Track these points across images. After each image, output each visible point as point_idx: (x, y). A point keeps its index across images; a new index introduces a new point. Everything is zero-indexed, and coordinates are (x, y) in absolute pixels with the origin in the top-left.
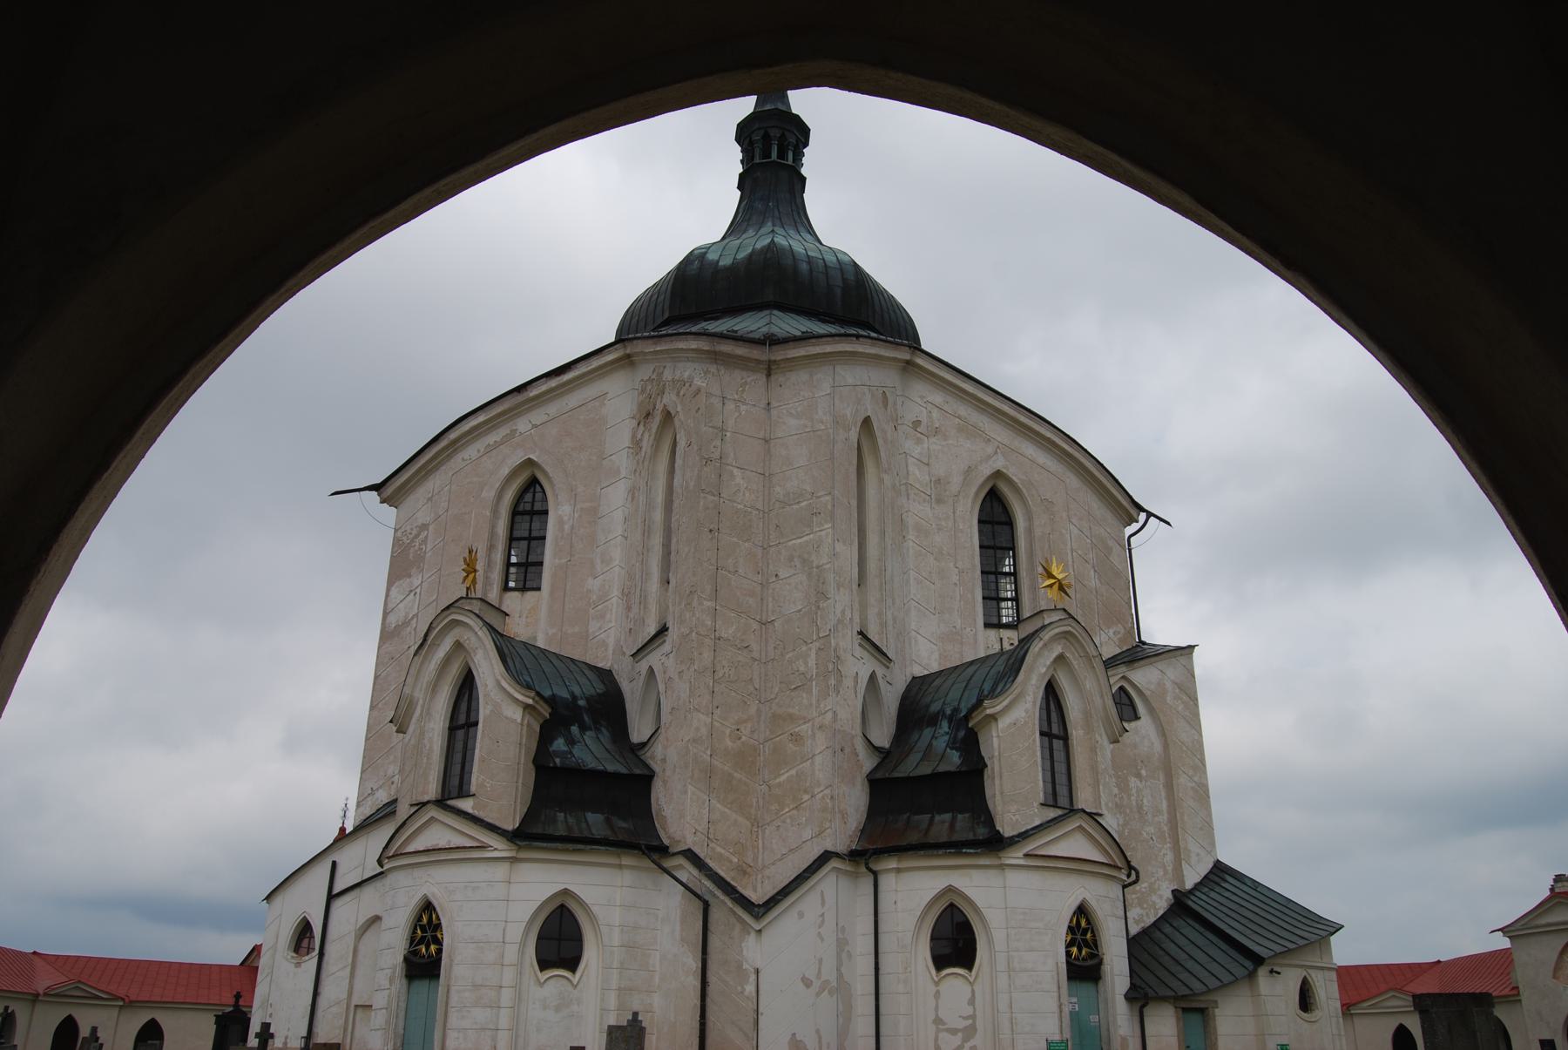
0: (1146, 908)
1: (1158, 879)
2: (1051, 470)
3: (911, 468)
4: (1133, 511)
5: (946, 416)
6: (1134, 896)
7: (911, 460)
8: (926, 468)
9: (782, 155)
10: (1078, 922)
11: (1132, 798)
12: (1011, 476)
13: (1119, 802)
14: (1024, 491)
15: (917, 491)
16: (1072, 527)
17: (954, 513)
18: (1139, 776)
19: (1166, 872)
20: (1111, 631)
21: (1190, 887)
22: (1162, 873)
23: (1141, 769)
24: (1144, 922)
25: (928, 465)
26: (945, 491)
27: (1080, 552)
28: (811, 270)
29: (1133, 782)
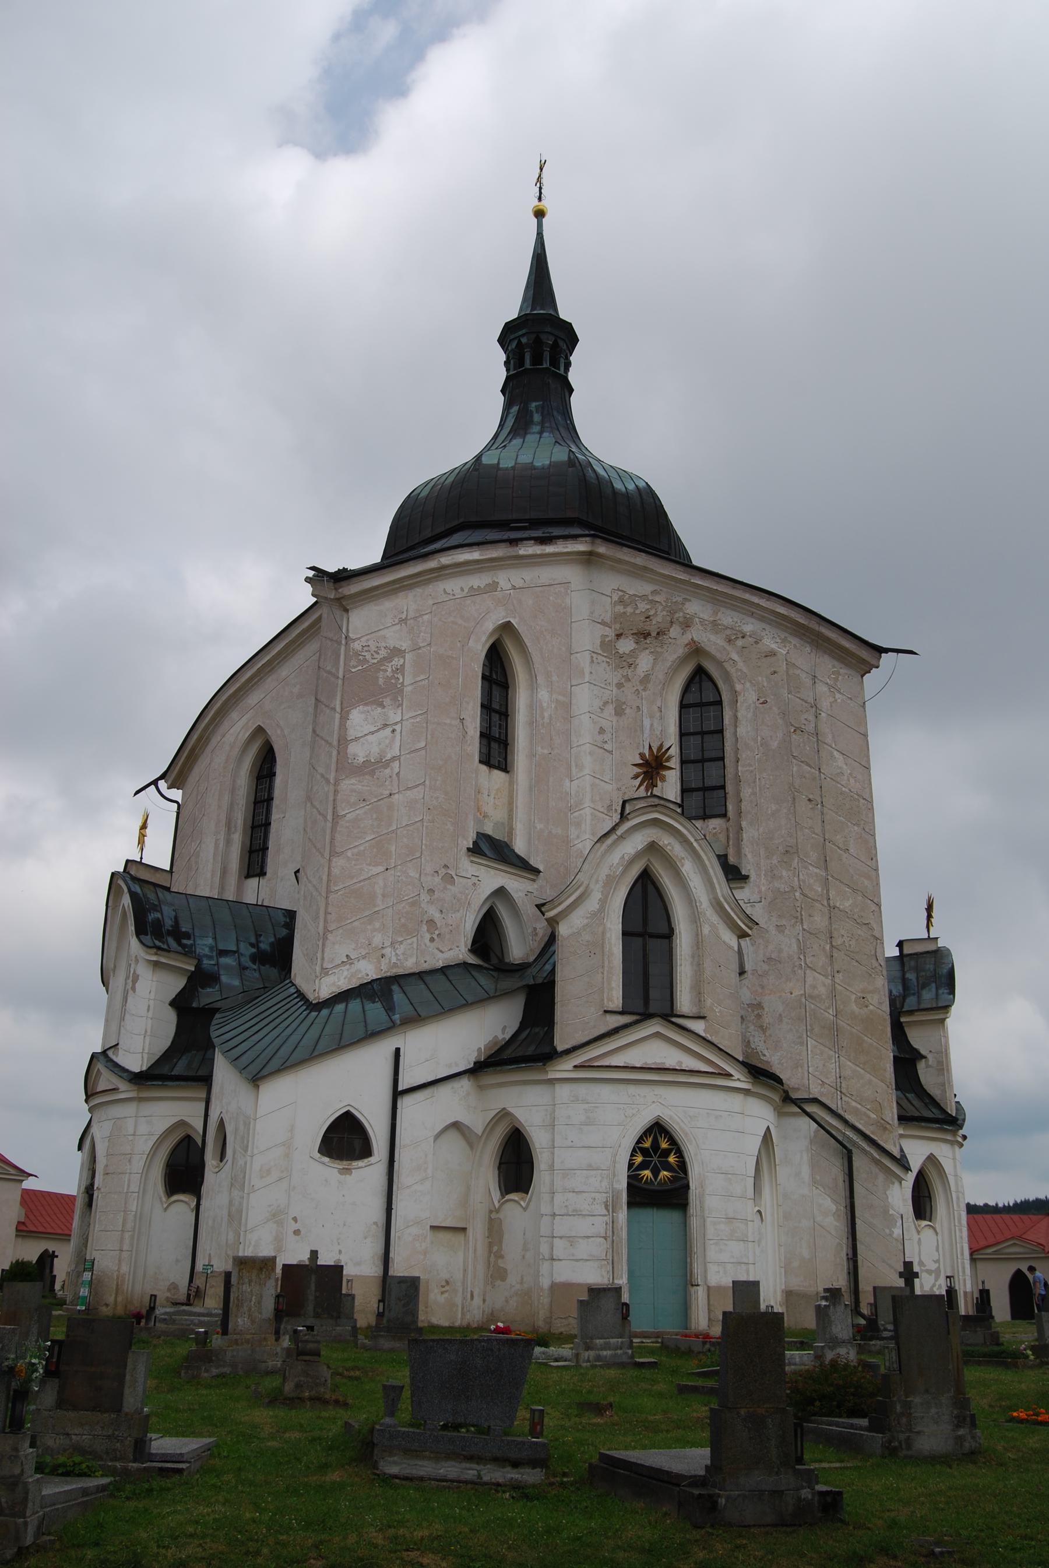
9: (537, 359)
10: (655, 1145)
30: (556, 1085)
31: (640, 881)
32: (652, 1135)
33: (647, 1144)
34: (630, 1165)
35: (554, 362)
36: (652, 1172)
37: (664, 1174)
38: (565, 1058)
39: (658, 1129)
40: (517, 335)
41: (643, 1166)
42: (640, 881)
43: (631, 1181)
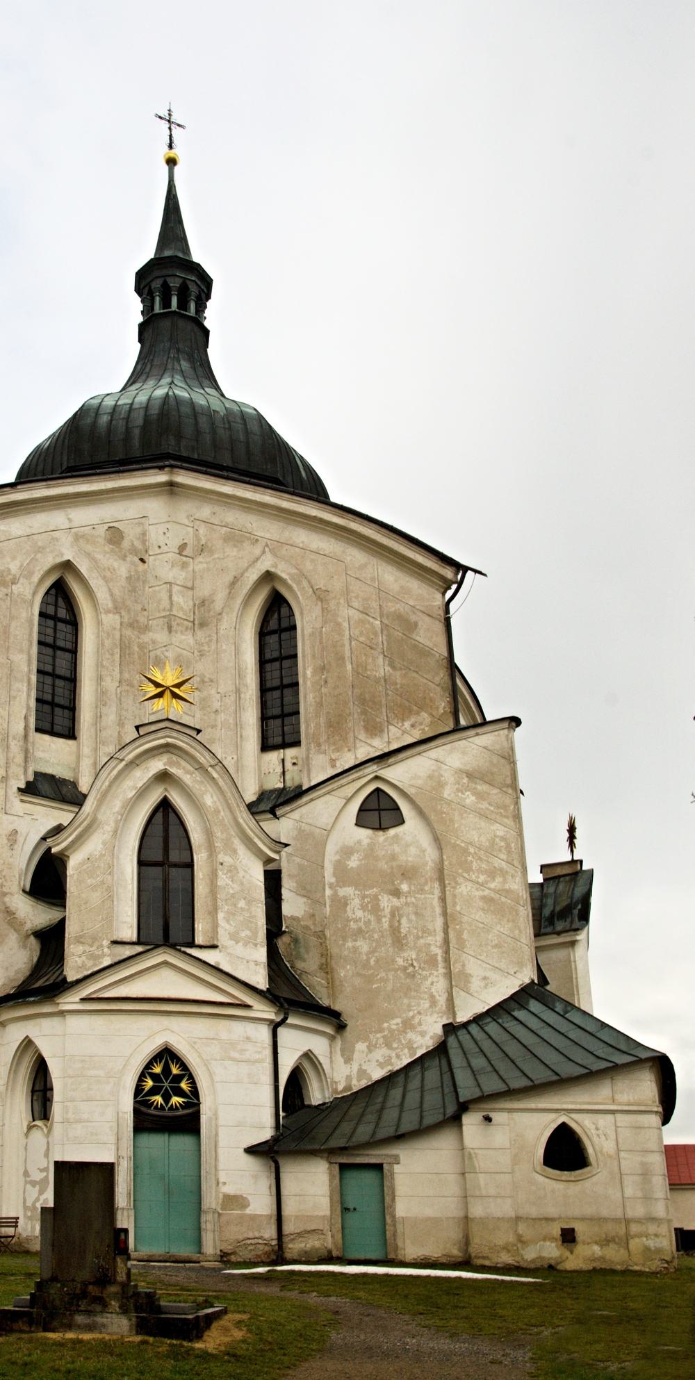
0: (396, 1048)
1: (419, 1013)
2: (326, 552)
3: (175, 598)
4: (448, 573)
5: (214, 530)
6: (379, 1035)
7: (175, 589)
8: (190, 593)
9: (166, 303)
10: (166, 1070)
11: (384, 920)
12: (279, 573)
13: (363, 927)
14: (294, 586)
15: (179, 621)
16: (352, 612)
17: (217, 633)
18: (397, 893)
19: (433, 1002)
20: (407, 724)
21: (465, 1020)
22: (427, 1005)
23: (400, 884)
24: (392, 1064)
25: (192, 589)
26: (209, 611)
27: (362, 639)
28: (111, 420)
29: (387, 902)
30: (67, 1017)
31: (161, 810)
32: (163, 1061)
33: (157, 1069)
34: (138, 1090)
35: (183, 304)
36: (163, 1097)
37: (176, 1100)
38: (74, 991)
39: (167, 1055)
40: (148, 280)
41: (154, 1091)
42: (161, 810)
43: (137, 1106)
